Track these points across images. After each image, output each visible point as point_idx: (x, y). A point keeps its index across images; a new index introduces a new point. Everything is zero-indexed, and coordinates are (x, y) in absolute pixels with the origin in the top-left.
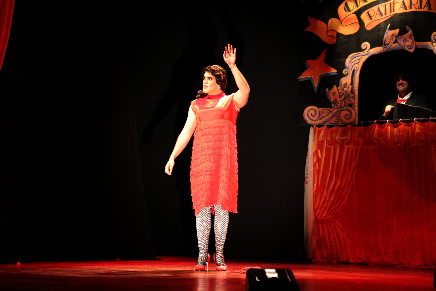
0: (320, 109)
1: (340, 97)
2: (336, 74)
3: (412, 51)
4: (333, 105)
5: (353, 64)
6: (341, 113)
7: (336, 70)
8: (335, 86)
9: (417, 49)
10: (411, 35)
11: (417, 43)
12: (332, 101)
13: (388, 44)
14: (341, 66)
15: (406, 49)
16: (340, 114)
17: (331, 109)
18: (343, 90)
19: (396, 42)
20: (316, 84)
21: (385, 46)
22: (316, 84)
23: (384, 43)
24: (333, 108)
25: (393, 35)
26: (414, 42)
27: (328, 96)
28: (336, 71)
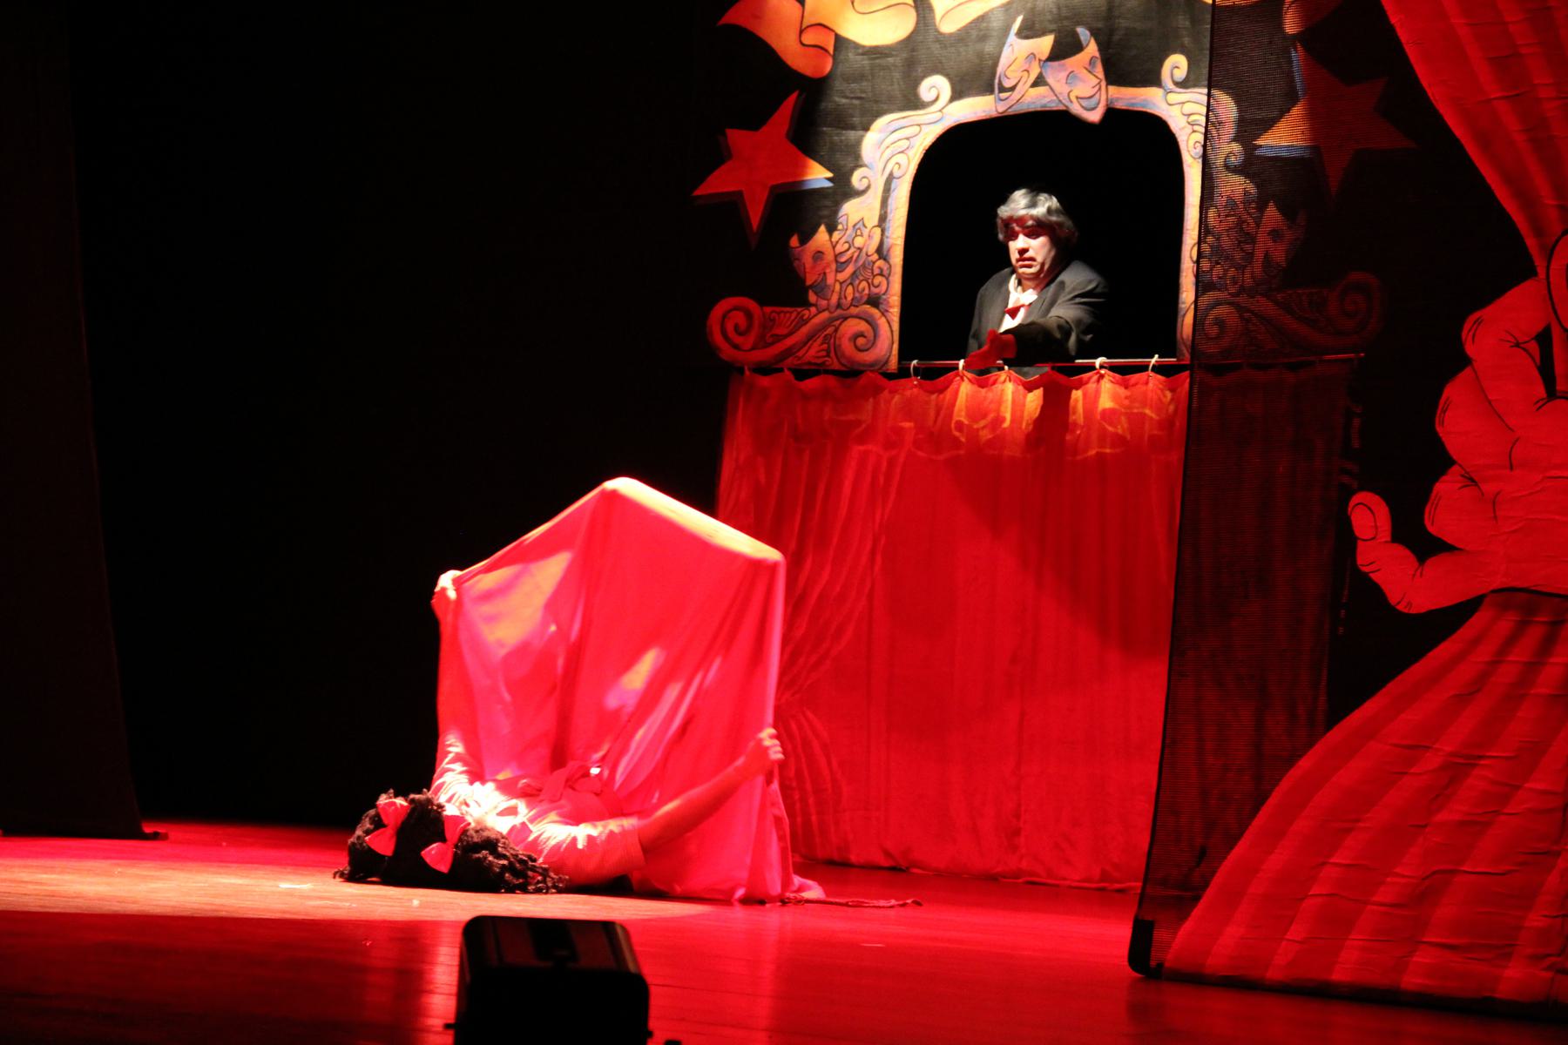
0: (768, 309)
2: (829, 184)
3: (1095, 116)
4: (812, 298)
5: (888, 153)
7: (829, 169)
8: (823, 228)
9: (1112, 113)
10: (1092, 61)
11: (1112, 89)
12: (808, 283)
13: (1013, 89)
15: (1076, 109)
16: (836, 330)
19: (1039, 82)
20: (755, 215)
21: (1004, 95)
22: (755, 215)
23: (1000, 83)
24: (813, 309)
25: (1032, 56)
26: (1104, 83)
27: (796, 263)
28: (830, 175)
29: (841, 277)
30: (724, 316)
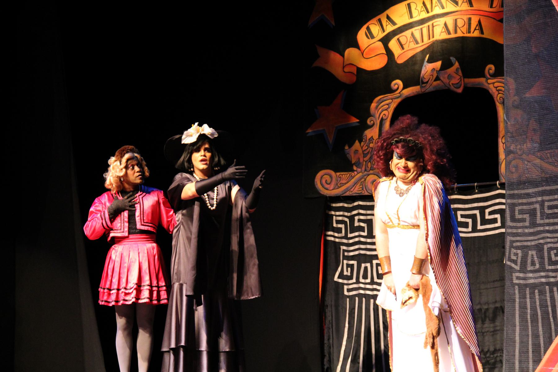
0: (338, 174)
1: (364, 157)
4: (355, 168)
5: (380, 110)
6: (367, 179)
8: (357, 141)
12: (353, 162)
13: (427, 82)
14: (364, 114)
16: (365, 180)
17: (353, 174)
18: (369, 147)
19: (437, 79)
24: (356, 173)
25: (433, 69)
28: (358, 121)
29: (366, 159)
30: (322, 178)
